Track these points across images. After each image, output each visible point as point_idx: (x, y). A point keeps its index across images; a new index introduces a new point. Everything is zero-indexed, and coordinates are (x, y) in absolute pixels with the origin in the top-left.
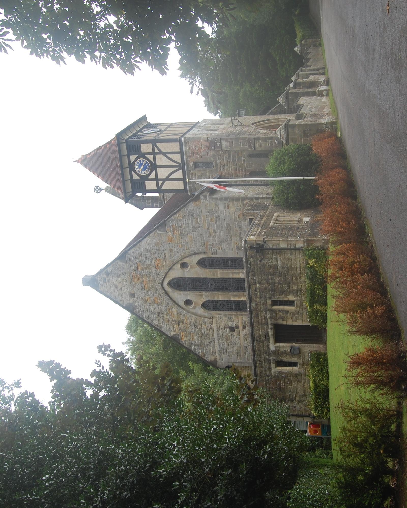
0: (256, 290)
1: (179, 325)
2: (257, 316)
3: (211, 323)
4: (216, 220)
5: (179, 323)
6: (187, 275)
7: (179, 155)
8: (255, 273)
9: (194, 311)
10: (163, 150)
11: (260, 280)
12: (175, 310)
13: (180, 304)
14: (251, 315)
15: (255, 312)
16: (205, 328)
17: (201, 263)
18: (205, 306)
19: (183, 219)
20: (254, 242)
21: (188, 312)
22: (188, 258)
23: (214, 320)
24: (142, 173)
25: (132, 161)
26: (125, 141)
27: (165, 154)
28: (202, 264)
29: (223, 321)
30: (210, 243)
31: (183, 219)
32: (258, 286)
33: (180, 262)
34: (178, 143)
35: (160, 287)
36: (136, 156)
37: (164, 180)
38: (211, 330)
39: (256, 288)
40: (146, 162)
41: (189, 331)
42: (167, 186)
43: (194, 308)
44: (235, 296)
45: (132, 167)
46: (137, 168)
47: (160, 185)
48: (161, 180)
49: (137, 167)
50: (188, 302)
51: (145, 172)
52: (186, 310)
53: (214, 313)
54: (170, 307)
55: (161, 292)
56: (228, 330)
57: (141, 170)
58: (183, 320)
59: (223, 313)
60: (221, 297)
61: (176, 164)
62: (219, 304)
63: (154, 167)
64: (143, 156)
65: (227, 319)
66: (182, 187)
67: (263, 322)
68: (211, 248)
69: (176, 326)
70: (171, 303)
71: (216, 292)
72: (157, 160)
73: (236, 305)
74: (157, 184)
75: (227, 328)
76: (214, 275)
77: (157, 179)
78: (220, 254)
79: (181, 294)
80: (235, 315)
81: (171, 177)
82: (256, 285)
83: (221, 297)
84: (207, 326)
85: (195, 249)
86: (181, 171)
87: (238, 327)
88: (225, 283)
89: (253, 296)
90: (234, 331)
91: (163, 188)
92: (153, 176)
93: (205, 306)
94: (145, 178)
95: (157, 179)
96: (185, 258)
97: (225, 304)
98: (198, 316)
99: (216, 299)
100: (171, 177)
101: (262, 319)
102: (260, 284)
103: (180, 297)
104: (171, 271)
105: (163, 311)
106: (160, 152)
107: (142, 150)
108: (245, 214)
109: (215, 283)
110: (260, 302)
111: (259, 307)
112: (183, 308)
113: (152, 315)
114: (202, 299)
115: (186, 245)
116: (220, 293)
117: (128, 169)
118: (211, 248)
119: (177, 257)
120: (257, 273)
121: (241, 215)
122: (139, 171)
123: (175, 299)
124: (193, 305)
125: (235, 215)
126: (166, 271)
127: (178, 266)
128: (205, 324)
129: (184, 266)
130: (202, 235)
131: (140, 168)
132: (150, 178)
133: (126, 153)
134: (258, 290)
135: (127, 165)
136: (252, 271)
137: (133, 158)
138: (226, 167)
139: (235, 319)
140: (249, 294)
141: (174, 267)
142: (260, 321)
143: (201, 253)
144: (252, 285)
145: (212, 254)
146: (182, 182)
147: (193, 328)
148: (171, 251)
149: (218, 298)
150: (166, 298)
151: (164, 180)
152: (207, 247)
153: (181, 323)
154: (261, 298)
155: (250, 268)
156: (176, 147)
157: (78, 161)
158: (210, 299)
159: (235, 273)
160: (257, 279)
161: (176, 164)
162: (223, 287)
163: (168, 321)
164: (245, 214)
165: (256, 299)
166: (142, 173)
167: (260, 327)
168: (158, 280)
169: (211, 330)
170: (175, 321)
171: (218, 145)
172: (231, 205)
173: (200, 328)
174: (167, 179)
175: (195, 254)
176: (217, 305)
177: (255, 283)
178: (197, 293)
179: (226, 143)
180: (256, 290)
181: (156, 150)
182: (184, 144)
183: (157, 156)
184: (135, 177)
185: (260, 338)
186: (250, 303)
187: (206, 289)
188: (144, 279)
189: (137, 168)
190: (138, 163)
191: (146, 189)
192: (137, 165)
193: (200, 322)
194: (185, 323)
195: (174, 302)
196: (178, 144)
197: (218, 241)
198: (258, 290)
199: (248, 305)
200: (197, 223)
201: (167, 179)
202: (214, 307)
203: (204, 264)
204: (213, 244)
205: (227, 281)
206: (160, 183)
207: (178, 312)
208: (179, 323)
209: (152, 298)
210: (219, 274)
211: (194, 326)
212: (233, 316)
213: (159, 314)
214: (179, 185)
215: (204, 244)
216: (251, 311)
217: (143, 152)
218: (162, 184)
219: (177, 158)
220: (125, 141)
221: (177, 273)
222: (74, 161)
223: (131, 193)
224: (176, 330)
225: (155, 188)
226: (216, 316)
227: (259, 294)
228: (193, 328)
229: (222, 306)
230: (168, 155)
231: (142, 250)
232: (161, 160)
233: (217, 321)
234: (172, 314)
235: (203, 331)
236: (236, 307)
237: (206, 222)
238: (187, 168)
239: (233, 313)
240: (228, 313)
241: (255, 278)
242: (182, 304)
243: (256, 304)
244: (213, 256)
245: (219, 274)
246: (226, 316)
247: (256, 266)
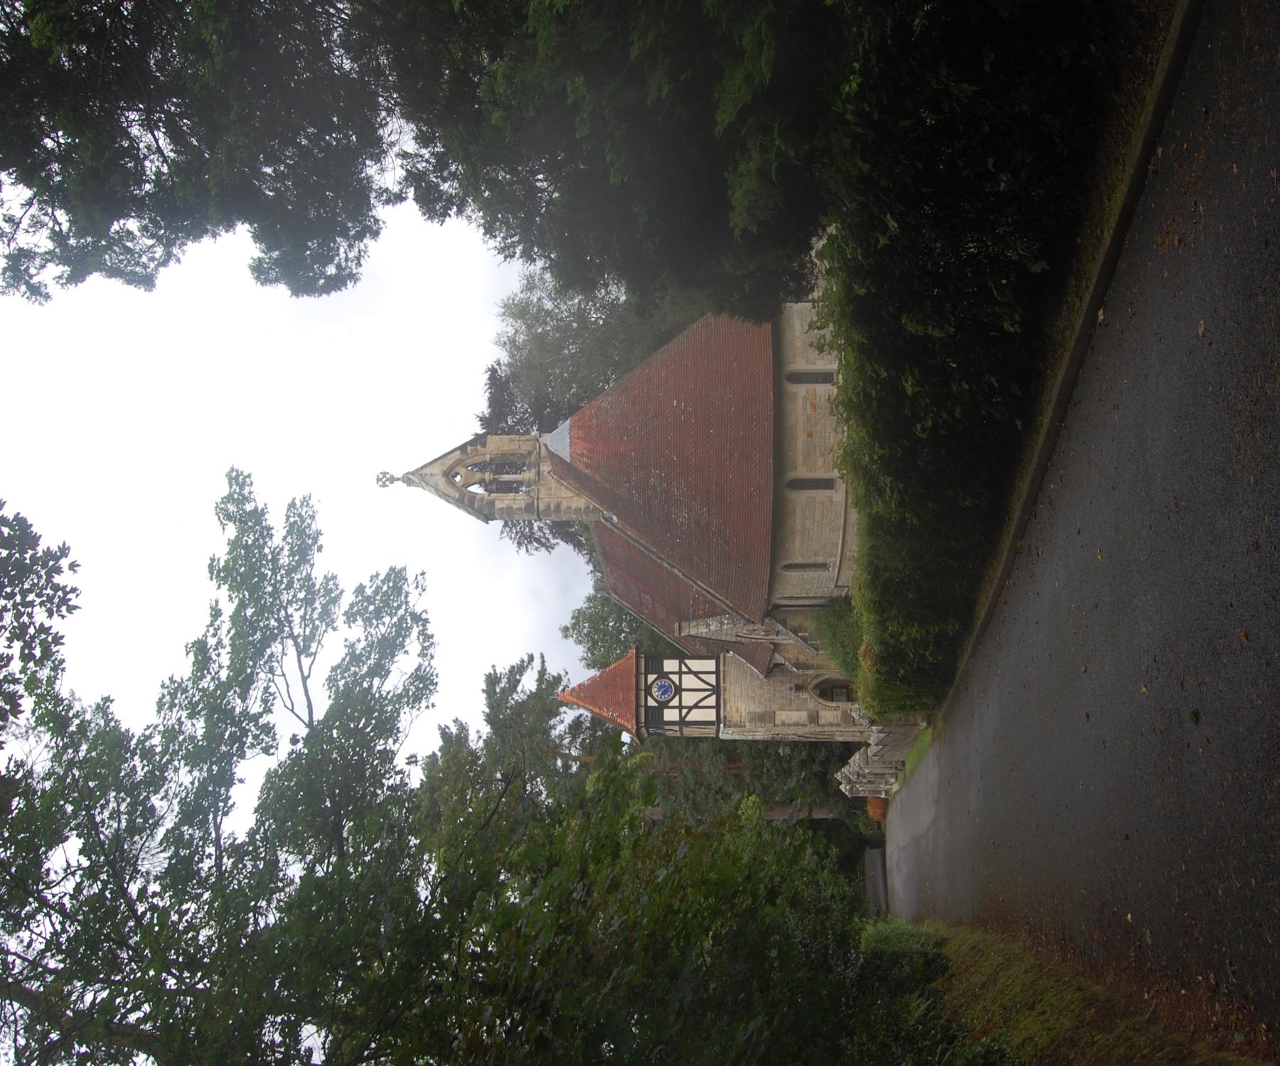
7: (714, 676)
27: (696, 674)
37: (690, 709)
42: (695, 716)
45: (648, 690)
63: (679, 690)
64: (665, 675)
66: (713, 718)
77: (680, 707)
91: (688, 719)
92: (675, 702)
94: (664, 705)
95: (680, 707)
106: (690, 672)
137: (651, 678)
146: (714, 711)
151: (690, 709)
156: (710, 665)
174: (696, 706)
181: (684, 669)
184: (651, 703)
196: (713, 662)
201: (696, 706)
206: (684, 711)
214: (711, 715)
218: (687, 714)
219: (712, 679)
225: (677, 719)
232: (689, 681)
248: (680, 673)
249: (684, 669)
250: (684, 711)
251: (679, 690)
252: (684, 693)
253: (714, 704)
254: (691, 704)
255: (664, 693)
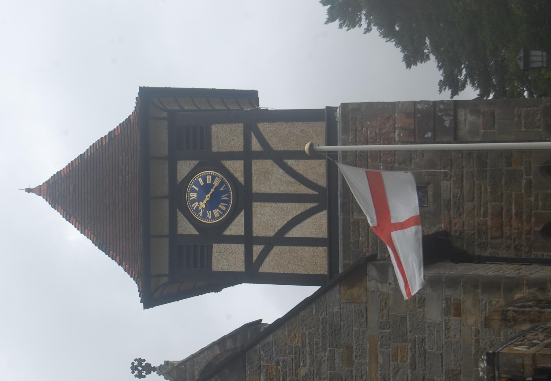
4: (413, 356)
10: (276, 145)
19: (304, 346)
20: (528, 362)
24: (205, 216)
25: (180, 177)
26: (165, 114)
27: (280, 158)
31: (304, 346)
34: (324, 124)
36: (194, 163)
37: (269, 243)
40: (222, 183)
46: (193, 201)
47: (255, 258)
48: (260, 240)
49: (194, 196)
51: (216, 212)
57: (203, 205)
61: (311, 192)
64: (215, 161)
72: (254, 178)
74: (248, 253)
77: (248, 239)
81: (295, 232)
86: (322, 217)
92: (237, 227)
94: (215, 233)
95: (248, 239)
100: (295, 232)
106: (268, 153)
107: (214, 142)
108: (510, 314)
117: (166, 202)
121: (497, 317)
122: (197, 210)
125: (478, 341)
131: (200, 199)
132: (228, 232)
133: (164, 150)
135: (165, 189)
138: (468, 206)
146: (322, 252)
151: (269, 243)
157: (38, 191)
161: (311, 192)
164: (510, 314)
166: (205, 216)
171: (447, 124)
172: (468, 303)
174: (281, 238)
179: (471, 118)
181: (256, 146)
182: (339, 126)
183: (257, 165)
184: (186, 228)
189: (193, 201)
190: (197, 183)
191: (215, 268)
192: (193, 191)
200: (349, 361)
206: (257, 249)
217: (215, 149)
218: (263, 255)
220: (165, 114)
222: (29, 190)
223: (165, 280)
230: (290, 163)
237: (380, 360)
238: (344, 204)
248: (247, 156)
249: (256, 146)
250: (257, 249)
251: (244, 198)
252: (258, 208)
253: (323, 233)
254: (271, 233)
255: (211, 205)
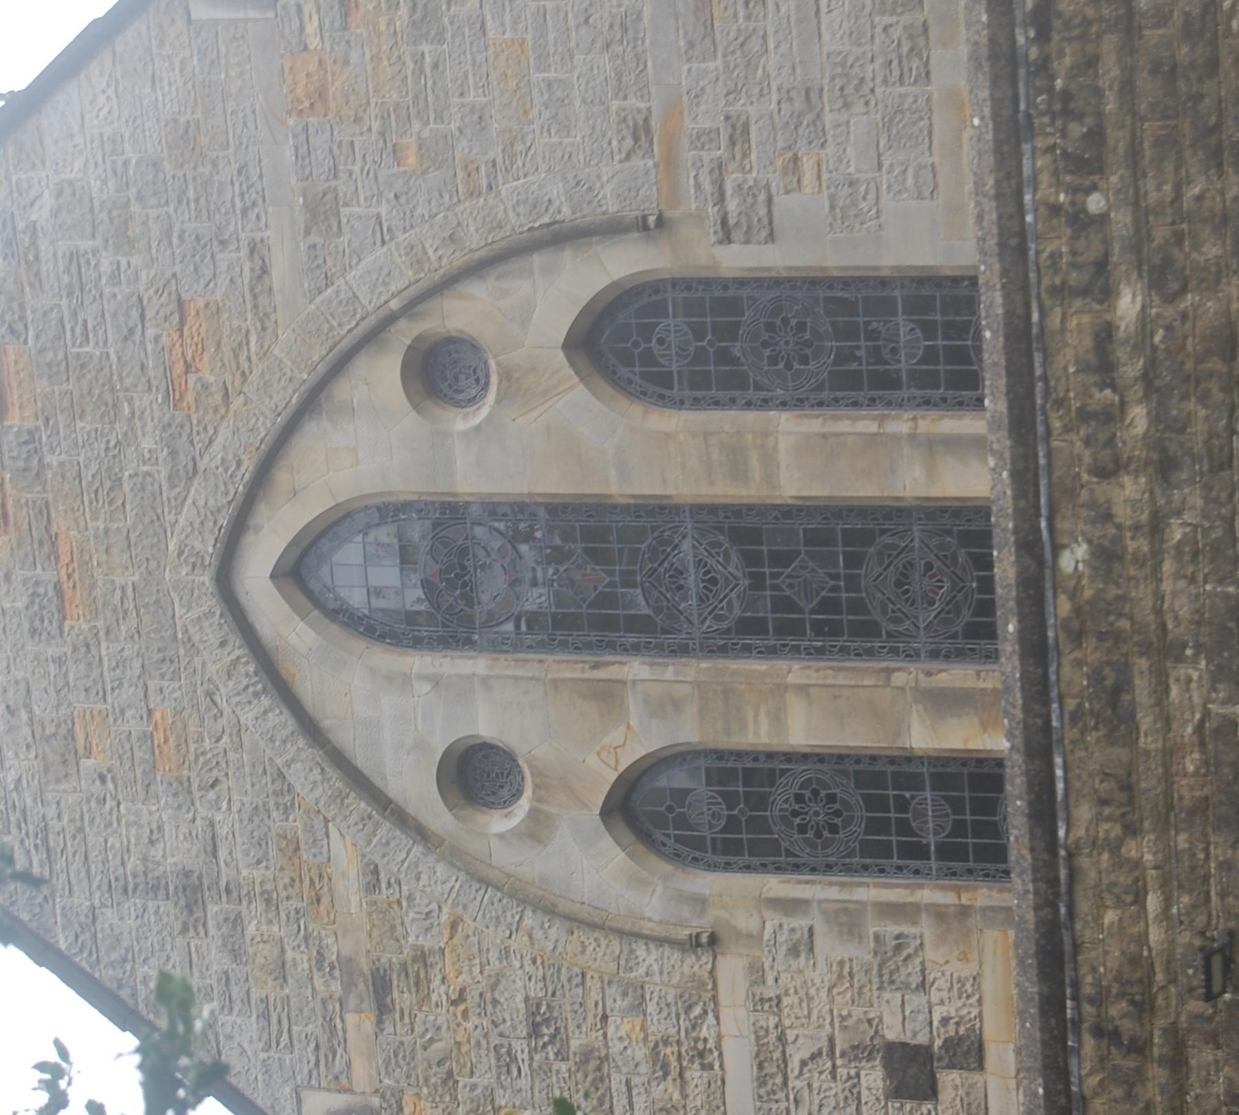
0: (1102, 363)
1: (383, 1010)
2: (1113, 709)
3: (700, 998)
5: (381, 986)
6: (471, 478)
8: (1096, 136)
9: (529, 864)
11: (1161, 233)
12: (344, 854)
13: (394, 787)
14: (1038, 690)
15: (1092, 651)
16: (640, 1053)
17: (620, 344)
18: (640, 809)
21: (480, 876)
22: (479, 290)
23: (732, 970)
28: (627, 360)
29: (820, 976)
30: (705, 116)
32: (1128, 304)
33: (405, 333)
35: (211, 602)
38: (694, 1074)
39: (1105, 335)
41: (484, 1079)
43: (536, 830)
44: (944, 702)
50: (476, 774)
52: (454, 856)
53: (734, 894)
54: (296, 822)
55: (216, 654)
56: (873, 1078)
58: (422, 957)
59: (821, 890)
60: (803, 709)
62: (781, 800)
65: (861, 954)
67: (1187, 791)
68: (719, 169)
69: (358, 1024)
70: (308, 777)
71: (759, 666)
73: (957, 805)
75: (858, 1052)
76: (738, 472)
78: (805, 242)
79: (404, 681)
80: (939, 914)
82: (1108, 294)
83: (803, 709)
84: (659, 1026)
85: (556, 191)
87: (968, 1051)
88: (853, 561)
89: (1069, 446)
90: (930, 1092)
93: (640, 809)
96: (450, 282)
97: (853, 796)
98: (573, 920)
99: (758, 734)
101: (1170, 754)
102: (1163, 278)
103: (405, 711)
104: (311, 429)
105: (238, 863)
109: (751, 559)
110: (1156, 527)
111: (1142, 593)
112: (421, 833)
113: (132, 905)
114: (616, 736)
115: (462, 146)
116: (796, 671)
118: (719, 169)
119: (374, 276)
120: (1118, 139)
123: (344, 738)
124: (524, 805)
126: (266, 427)
127: (381, 377)
128: (639, 1006)
129: (441, 372)
130: (627, 25)
134: (1131, 369)
136: (1066, 107)
139: (940, 958)
140: (1023, 425)
141: (347, 389)
142: (1149, 782)
143: (612, 229)
144: (1061, 292)
145: (727, 237)
147: (520, 1047)
148: (321, 212)
149: (778, 719)
150: (262, 718)
152: (670, 163)
153: (402, 997)
154: (1164, 468)
155: (1043, 67)
158: (688, 731)
159: (953, 444)
160: (1122, 221)
162: (829, 605)
163: (281, 971)
165: (1103, 490)
167: (1144, 850)
168: (193, 523)
169: (694, 1074)
170: (346, 964)
173: (586, 1056)
175: (558, 237)
176: (762, 802)
177: (1102, 265)
178: (569, 668)
180: (1102, 363)
185: (1144, 1007)
186: (1029, 545)
187: (656, 634)
188: (61, 524)
193: (593, 985)
194: (439, 992)
195: (338, 759)
197: (786, 96)
198: (1131, 369)
199: (1006, 568)
202: (732, 824)
203: (648, 358)
204: (739, 133)
205: (866, 538)
207: (373, 878)
208: (381, 986)
209: (133, 724)
210: (796, 455)
211: (535, 1030)
212: (926, 928)
213: (192, 893)
215: (641, 132)
216: (1036, 651)
221: (373, 447)
224: (362, 1073)
226: (745, 921)
227: (1139, 417)
228: (521, 1047)
229: (817, 813)
231: (42, 213)
233: (756, 973)
234: (318, 888)
235: (616, 1082)
236: (959, 828)
239: (929, 895)
240: (871, 892)
241: (1095, 203)
242: (414, 783)
243: (1107, 557)
244: (735, 259)
245: (796, 455)
246: (847, 921)
247: (1109, 45)
